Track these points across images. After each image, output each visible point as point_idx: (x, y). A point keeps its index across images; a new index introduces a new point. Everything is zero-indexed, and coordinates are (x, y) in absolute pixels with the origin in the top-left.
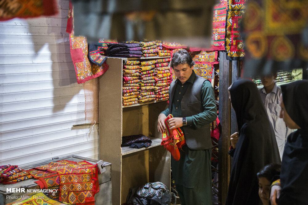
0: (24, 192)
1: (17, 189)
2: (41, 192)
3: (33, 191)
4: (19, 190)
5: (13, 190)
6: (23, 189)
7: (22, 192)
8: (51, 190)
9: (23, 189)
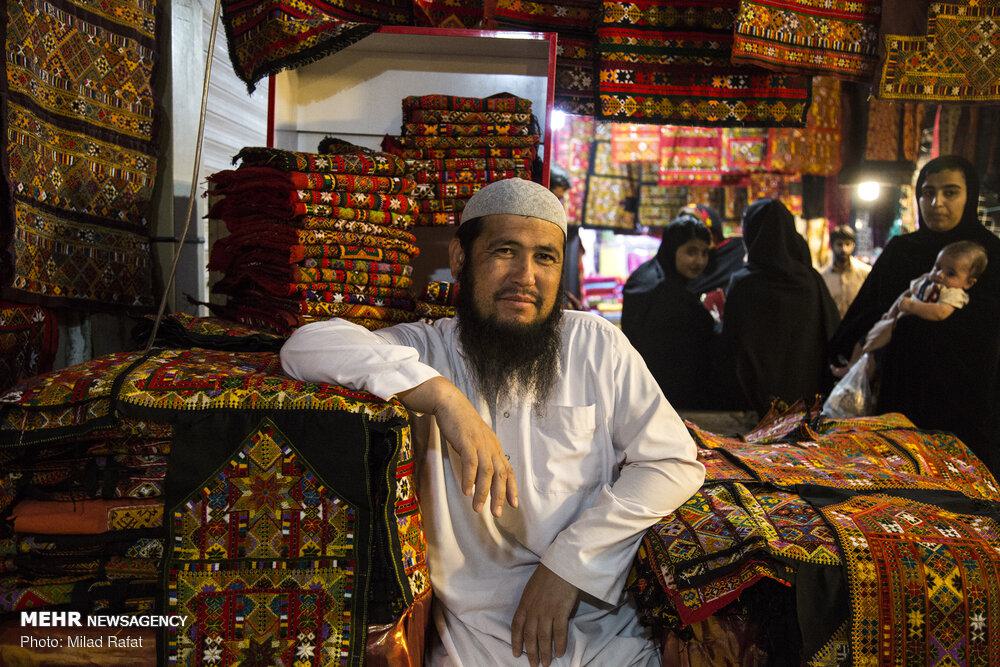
0: (79, 624)
1: (55, 614)
2: (134, 625)
3: (106, 623)
4: (63, 618)
5: (42, 619)
6: (74, 617)
7: (70, 624)
8: (165, 618)
9: (74, 617)
